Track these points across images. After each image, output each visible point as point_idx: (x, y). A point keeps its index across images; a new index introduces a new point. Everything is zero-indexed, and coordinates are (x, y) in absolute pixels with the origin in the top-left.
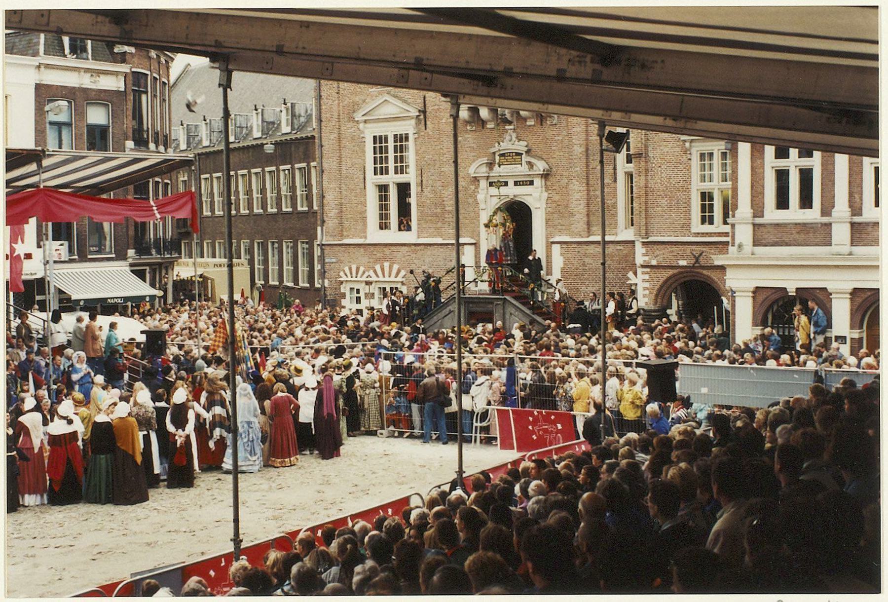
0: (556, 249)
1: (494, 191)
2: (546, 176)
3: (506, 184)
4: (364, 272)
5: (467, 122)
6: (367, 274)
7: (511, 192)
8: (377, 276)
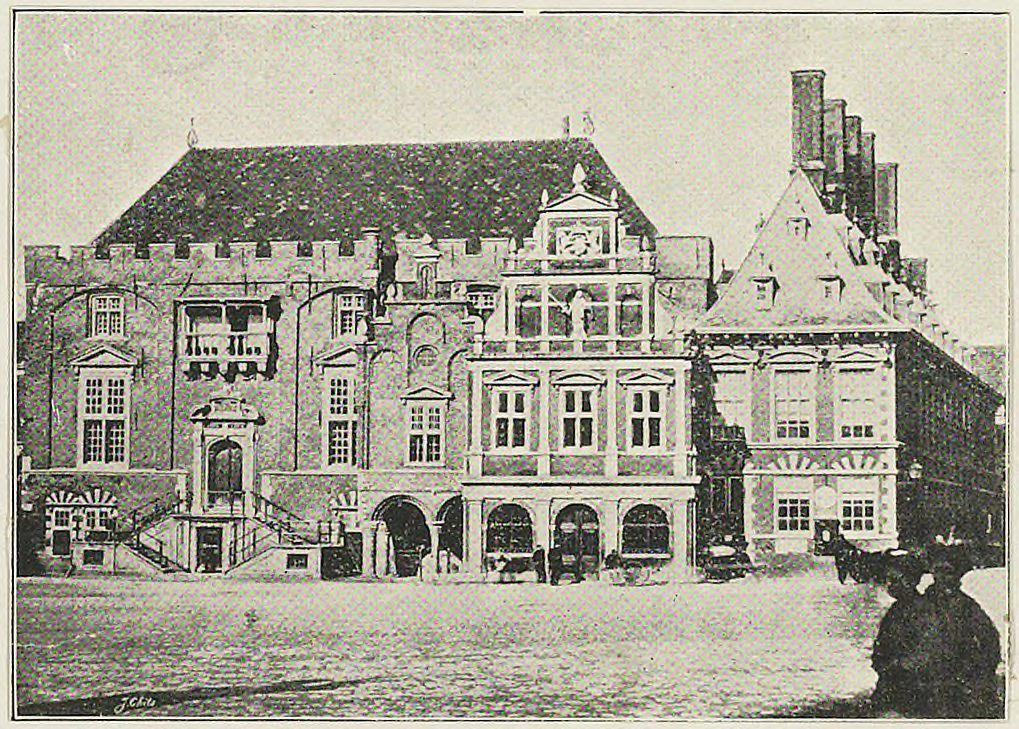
0: (266, 480)
1: (207, 431)
2: (261, 421)
3: (221, 426)
4: (70, 501)
5: (186, 373)
6: (76, 499)
7: (225, 432)
8: (87, 501)
